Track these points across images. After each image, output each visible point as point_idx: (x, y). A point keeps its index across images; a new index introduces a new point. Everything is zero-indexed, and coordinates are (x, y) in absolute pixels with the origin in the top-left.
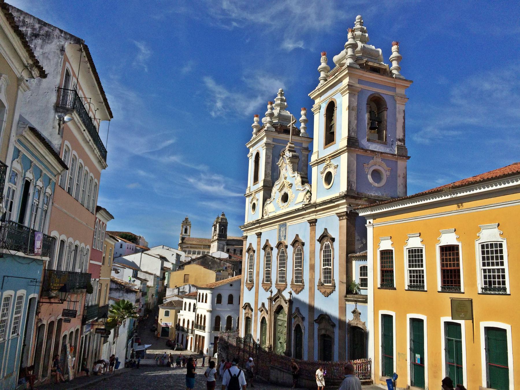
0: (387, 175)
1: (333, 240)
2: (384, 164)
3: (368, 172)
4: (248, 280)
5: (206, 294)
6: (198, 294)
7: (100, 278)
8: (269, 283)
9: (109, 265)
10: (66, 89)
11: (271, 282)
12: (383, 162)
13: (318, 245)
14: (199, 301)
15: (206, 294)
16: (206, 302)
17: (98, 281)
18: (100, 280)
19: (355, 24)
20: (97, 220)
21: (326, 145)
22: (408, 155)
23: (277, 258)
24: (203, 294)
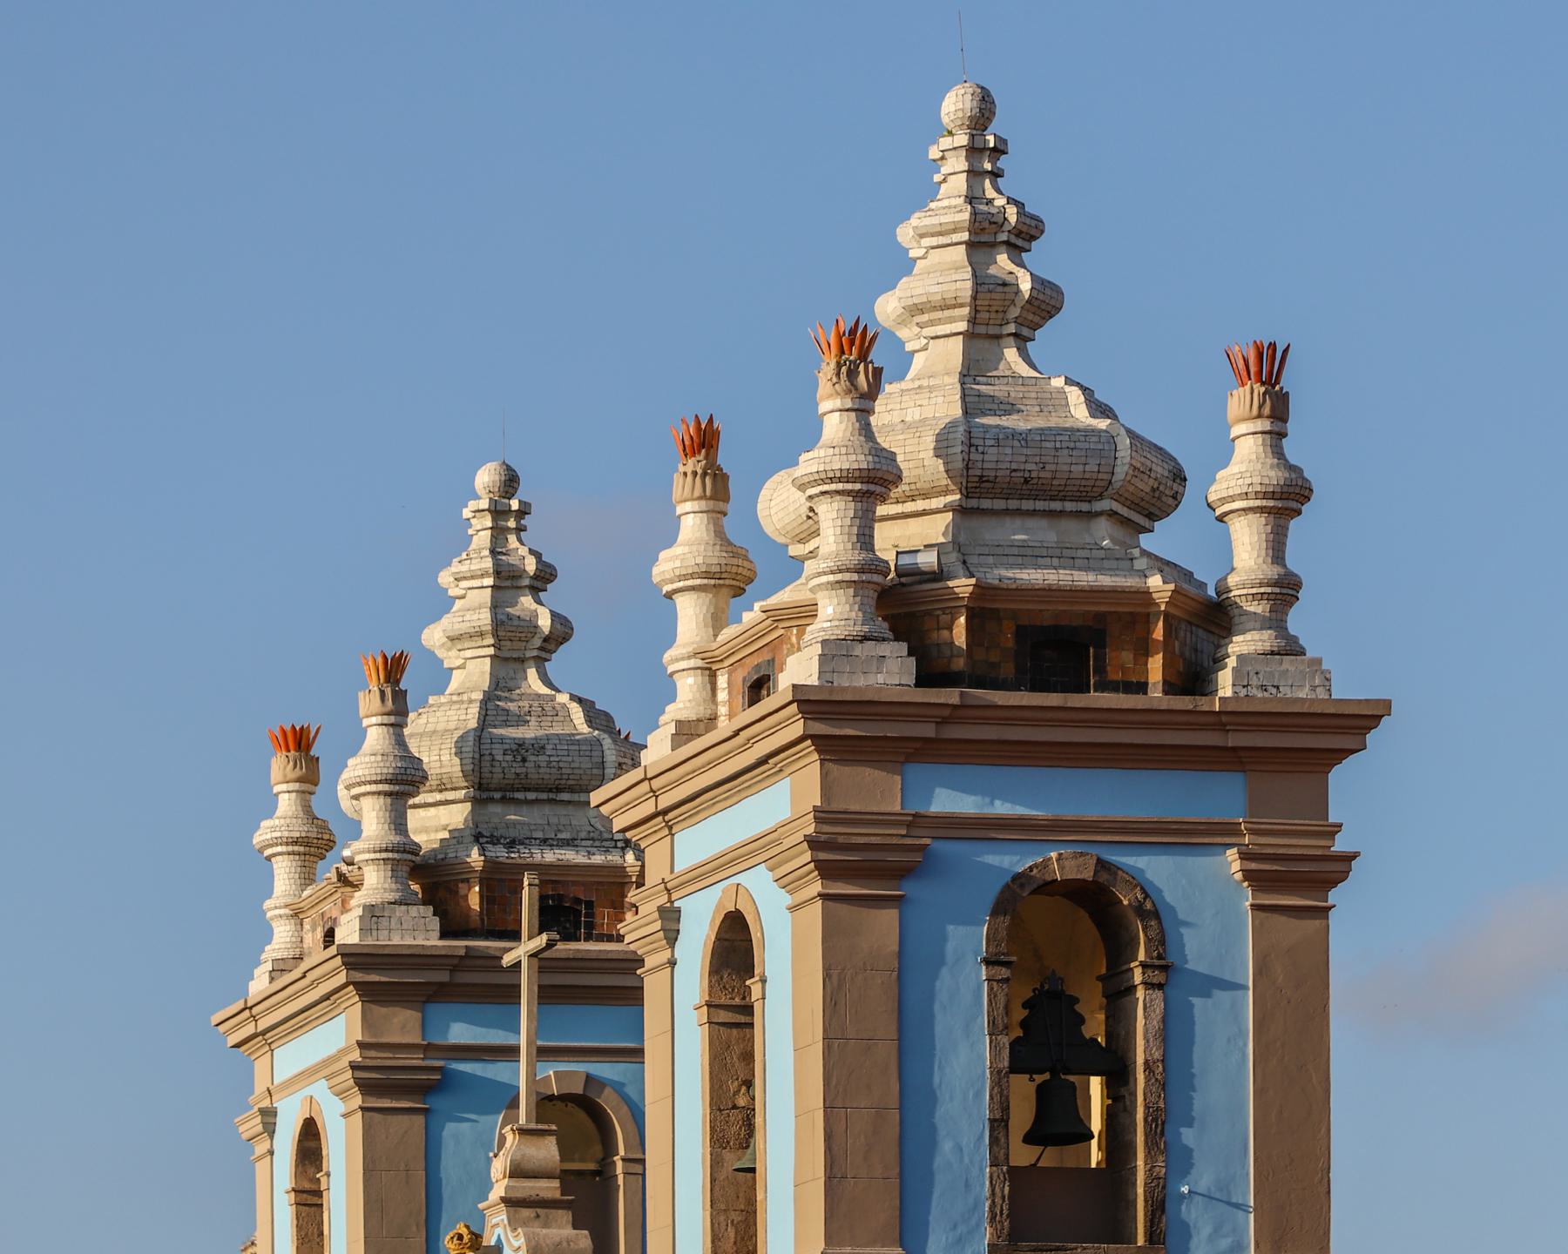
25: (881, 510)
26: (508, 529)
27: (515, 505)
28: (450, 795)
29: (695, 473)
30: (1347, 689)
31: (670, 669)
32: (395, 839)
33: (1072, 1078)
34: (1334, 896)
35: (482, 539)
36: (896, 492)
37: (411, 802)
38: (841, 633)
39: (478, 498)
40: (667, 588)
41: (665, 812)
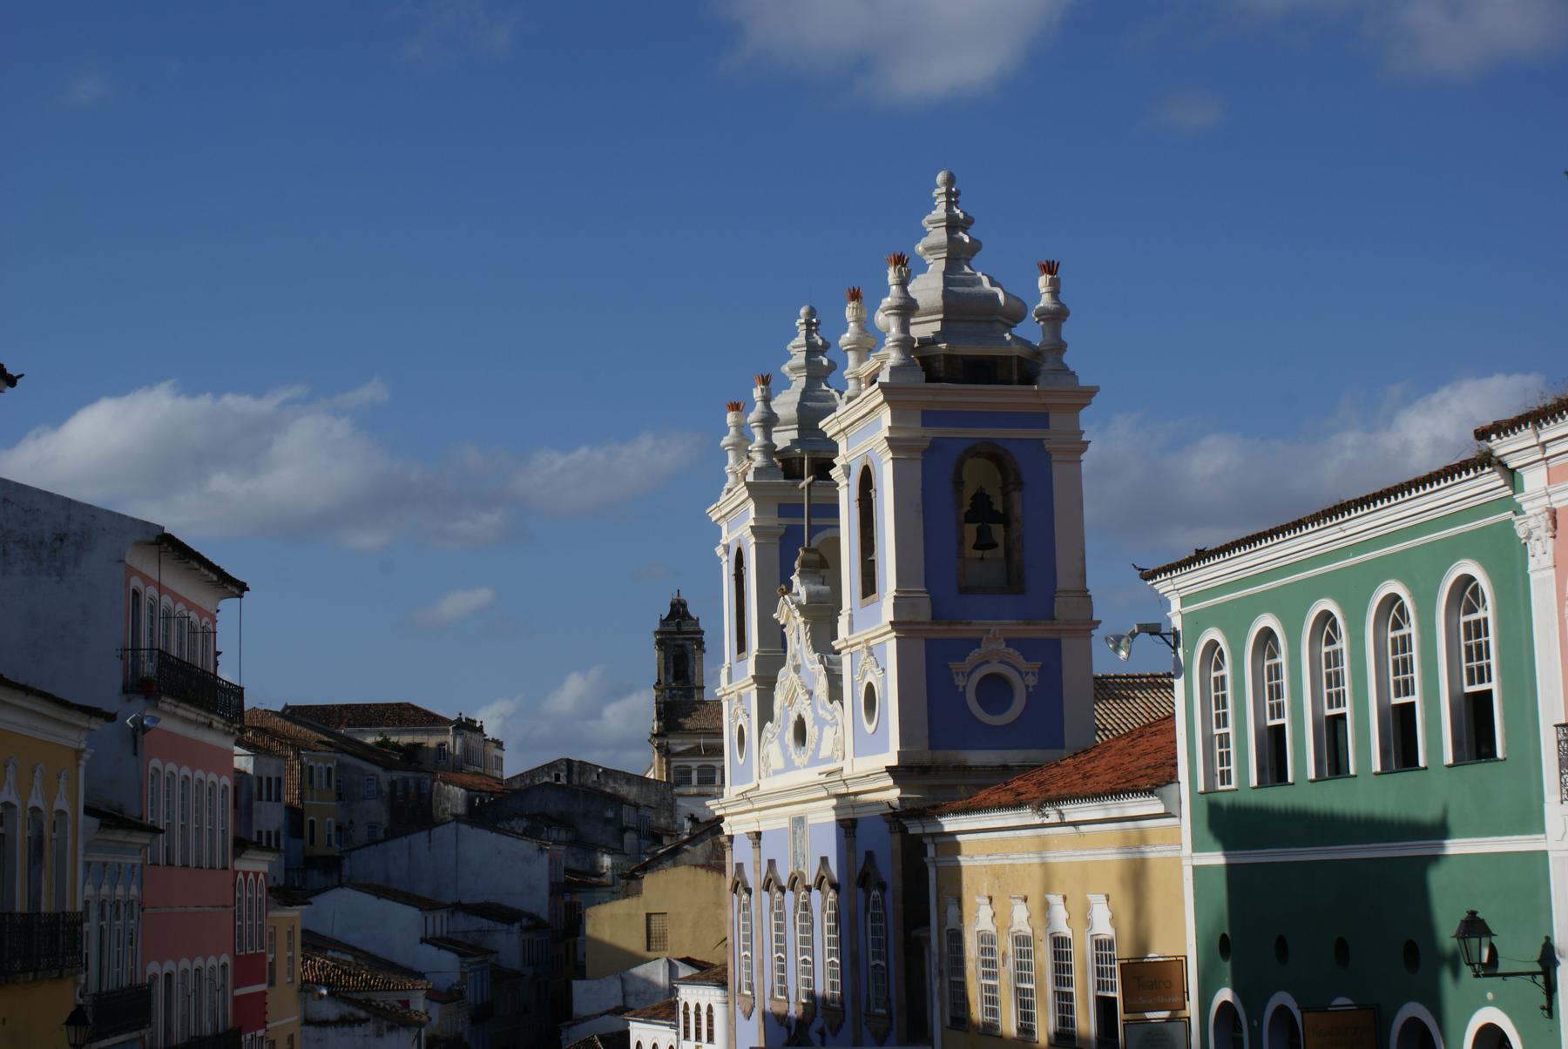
0: (1027, 687)
1: (882, 887)
2: (1017, 653)
3: (964, 687)
4: (743, 986)
5: (710, 1008)
6: (681, 1009)
7: (268, 1026)
8: (784, 998)
9: (289, 980)
10: (136, 649)
11: (788, 997)
12: (1011, 650)
13: (860, 890)
14: (686, 1036)
15: (710, 1008)
16: (710, 1039)
17: (262, 1037)
18: (267, 1031)
19: (935, 199)
20: (241, 876)
21: (863, 598)
22: (1095, 618)
23: (795, 923)
24: (698, 1007)
25: (912, 320)
26: (812, 330)
27: (814, 320)
28: (790, 427)
29: (853, 308)
30: (1084, 381)
31: (846, 377)
32: (765, 442)
33: (989, 524)
34: (1082, 457)
35: (802, 333)
36: (917, 313)
37: (774, 429)
38: (896, 364)
39: (800, 318)
40: (844, 348)
41: (843, 430)
